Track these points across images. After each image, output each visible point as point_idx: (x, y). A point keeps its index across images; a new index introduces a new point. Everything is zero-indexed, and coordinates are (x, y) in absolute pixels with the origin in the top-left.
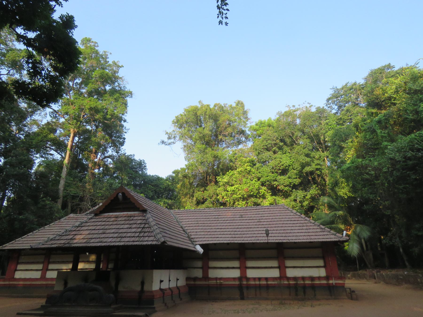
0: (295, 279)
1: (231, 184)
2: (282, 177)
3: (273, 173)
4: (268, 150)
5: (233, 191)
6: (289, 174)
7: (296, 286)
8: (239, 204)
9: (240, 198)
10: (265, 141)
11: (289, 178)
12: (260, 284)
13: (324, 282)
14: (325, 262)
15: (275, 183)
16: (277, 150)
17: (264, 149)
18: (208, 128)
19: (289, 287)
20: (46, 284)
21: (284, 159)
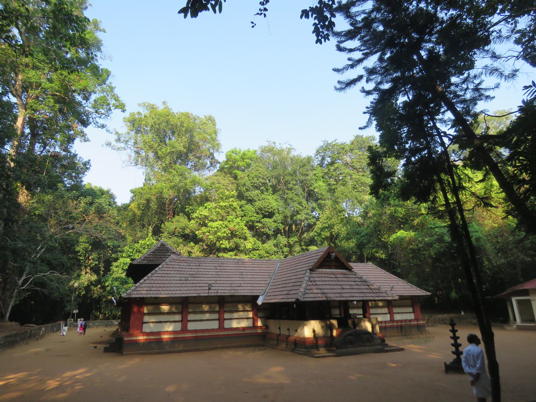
0: (401, 321)
1: (210, 219)
2: (267, 220)
3: (258, 213)
4: (257, 188)
5: (217, 228)
6: (274, 218)
7: (401, 326)
8: (222, 244)
9: (224, 236)
11: (275, 221)
13: (416, 323)
15: (258, 224)
16: (265, 190)
17: (252, 186)
18: (178, 143)
19: (397, 327)
20: (196, 337)
21: (272, 201)
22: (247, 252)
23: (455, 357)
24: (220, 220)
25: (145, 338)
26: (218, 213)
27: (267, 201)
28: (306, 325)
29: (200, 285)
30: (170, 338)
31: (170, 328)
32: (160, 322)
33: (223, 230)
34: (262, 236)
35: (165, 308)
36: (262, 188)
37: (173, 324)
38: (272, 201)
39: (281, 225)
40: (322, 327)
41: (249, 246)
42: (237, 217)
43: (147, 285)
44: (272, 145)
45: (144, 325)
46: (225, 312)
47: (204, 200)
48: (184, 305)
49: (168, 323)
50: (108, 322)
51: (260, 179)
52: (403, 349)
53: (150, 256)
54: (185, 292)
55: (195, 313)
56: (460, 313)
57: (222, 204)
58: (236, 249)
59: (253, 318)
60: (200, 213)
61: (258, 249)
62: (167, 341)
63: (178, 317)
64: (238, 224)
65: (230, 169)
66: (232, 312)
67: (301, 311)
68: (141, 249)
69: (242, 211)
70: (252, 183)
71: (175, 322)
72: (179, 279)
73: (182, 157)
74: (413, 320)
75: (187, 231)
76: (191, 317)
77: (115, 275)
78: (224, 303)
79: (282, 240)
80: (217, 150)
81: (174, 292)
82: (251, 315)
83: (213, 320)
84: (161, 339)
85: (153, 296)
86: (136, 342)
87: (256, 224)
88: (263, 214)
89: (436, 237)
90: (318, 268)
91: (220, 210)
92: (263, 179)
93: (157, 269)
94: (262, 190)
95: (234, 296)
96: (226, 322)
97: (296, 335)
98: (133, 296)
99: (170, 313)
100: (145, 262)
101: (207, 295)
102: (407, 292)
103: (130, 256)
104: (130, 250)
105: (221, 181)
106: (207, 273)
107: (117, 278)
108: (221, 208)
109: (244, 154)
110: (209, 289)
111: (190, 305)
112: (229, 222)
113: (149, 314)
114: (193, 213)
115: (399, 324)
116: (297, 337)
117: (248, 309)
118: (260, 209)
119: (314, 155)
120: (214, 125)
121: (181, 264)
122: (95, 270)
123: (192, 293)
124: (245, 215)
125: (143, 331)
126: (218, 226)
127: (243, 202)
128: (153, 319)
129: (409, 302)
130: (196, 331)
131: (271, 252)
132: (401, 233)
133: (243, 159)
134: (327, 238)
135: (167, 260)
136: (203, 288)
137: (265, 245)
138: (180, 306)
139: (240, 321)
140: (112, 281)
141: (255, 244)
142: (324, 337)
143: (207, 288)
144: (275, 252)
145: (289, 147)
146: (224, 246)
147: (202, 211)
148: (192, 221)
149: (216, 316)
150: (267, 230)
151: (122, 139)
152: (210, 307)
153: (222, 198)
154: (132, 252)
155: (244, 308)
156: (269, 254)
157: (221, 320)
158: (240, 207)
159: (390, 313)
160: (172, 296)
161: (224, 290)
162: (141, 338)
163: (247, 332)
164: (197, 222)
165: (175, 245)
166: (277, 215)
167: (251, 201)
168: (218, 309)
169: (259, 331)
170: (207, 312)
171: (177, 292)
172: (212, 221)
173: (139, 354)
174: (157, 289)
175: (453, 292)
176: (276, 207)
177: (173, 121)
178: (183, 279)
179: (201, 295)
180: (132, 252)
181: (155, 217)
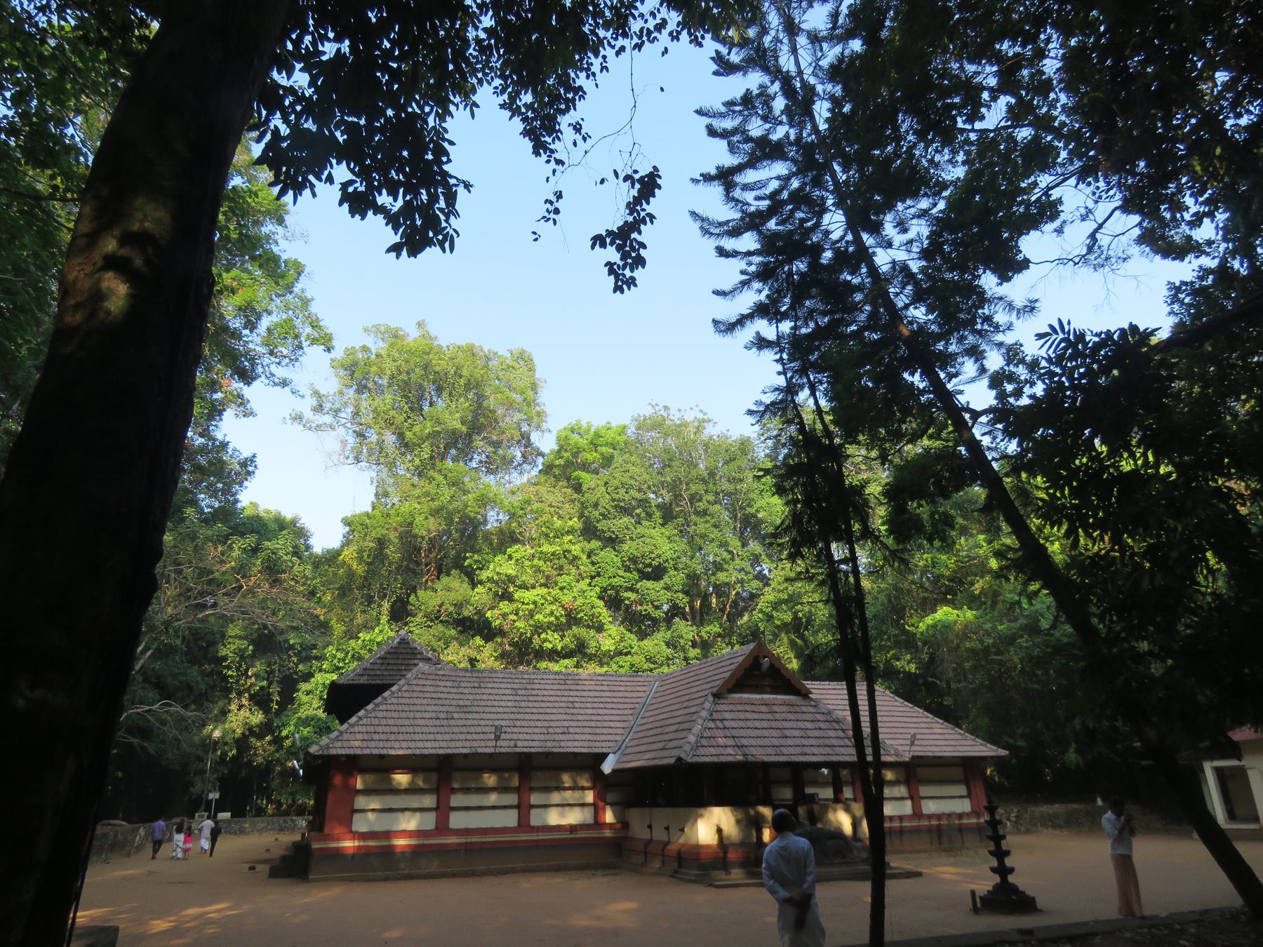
0: (939, 817)
1: (518, 583)
2: (649, 584)
3: (628, 569)
4: (626, 511)
5: (535, 603)
6: (666, 579)
7: (939, 829)
8: (545, 640)
9: (550, 623)
10: (622, 491)
11: (667, 588)
12: (960, 825)
13: (974, 821)
14: (909, 790)
15: (629, 594)
16: (643, 515)
17: (615, 507)
18: (449, 413)
19: (929, 830)
20: (466, 844)
21: (659, 541)
22: (603, 658)
23: (997, 879)
24: (541, 585)
25: (357, 843)
26: (538, 570)
27: (648, 540)
28: (701, 816)
29: (479, 729)
30: (409, 846)
31: (410, 823)
32: (391, 810)
33: (549, 608)
34: (639, 623)
35: (402, 779)
36: (638, 511)
37: (418, 815)
38: (659, 541)
39: (681, 595)
40: (738, 822)
41: (608, 644)
42: (580, 578)
43: (364, 729)
44: (662, 412)
45: (356, 817)
46: (532, 789)
47: (507, 539)
48: (444, 773)
49: (407, 814)
50: (285, 822)
51: (632, 492)
52: (919, 874)
53: (376, 667)
54: (445, 745)
55: (466, 791)
56: (1095, 801)
57: (547, 548)
58: (580, 651)
59: (594, 805)
60: (498, 570)
61: (626, 654)
62: (403, 853)
63: (429, 801)
64: (582, 594)
65: (566, 468)
66: (547, 790)
67: (688, 785)
68: (362, 652)
69: (593, 564)
70: (614, 500)
71: (421, 810)
72: (433, 715)
73: (458, 443)
74: (968, 815)
75: (467, 612)
76: (457, 800)
77: (304, 713)
78: (532, 771)
79: (686, 630)
80: (538, 427)
81: (420, 744)
82: (589, 797)
83: (505, 807)
84: (392, 847)
85: (375, 752)
86: (338, 854)
87: (626, 594)
88: (639, 571)
89: (1022, 621)
90: (731, 691)
91: (541, 563)
92: (639, 490)
93: (386, 694)
94: (638, 515)
95: (552, 753)
96: (533, 812)
97: (681, 841)
98: (333, 752)
99: (411, 790)
100: (363, 680)
101: (492, 750)
102: (950, 749)
103: (338, 668)
104: (340, 655)
105: (545, 496)
106: (496, 703)
107: (307, 718)
108: (544, 557)
109: (597, 435)
110: (497, 738)
111: (456, 775)
112: (562, 589)
113: (367, 792)
114: (481, 569)
115: (935, 822)
116: (683, 845)
117: (585, 784)
118: (633, 560)
119: (755, 435)
120: (532, 369)
121: (442, 684)
122: (260, 700)
123: (461, 747)
124: (599, 575)
125: (354, 829)
126: (537, 599)
127: (595, 544)
128: (375, 804)
129: (958, 772)
130: (467, 832)
131: (660, 659)
132: (944, 613)
133: (594, 445)
134: (785, 625)
135: (409, 676)
136: (485, 736)
137: (645, 642)
138: (434, 776)
139: (565, 812)
140: (296, 726)
141: (622, 640)
142: (743, 844)
143: (492, 736)
144: (668, 659)
145: (700, 416)
146: (550, 646)
147: (501, 566)
148: (479, 589)
149: (512, 799)
150: (650, 608)
151: (327, 406)
152: (500, 779)
153: (547, 535)
154: (344, 660)
155: (575, 782)
156: (654, 663)
157: (523, 809)
158: (589, 556)
159: (911, 798)
160: (418, 752)
161: (529, 740)
162: (349, 844)
163: (580, 835)
164: (490, 589)
165: (441, 643)
166: (672, 572)
167: (612, 542)
168: (517, 784)
169: (608, 833)
170: (493, 789)
171: (428, 744)
172: (524, 587)
173: (342, 879)
174: (384, 737)
175: (1072, 750)
176: (669, 554)
177: (439, 365)
178: (441, 716)
179: (480, 750)
180: (344, 660)
181: (396, 580)
